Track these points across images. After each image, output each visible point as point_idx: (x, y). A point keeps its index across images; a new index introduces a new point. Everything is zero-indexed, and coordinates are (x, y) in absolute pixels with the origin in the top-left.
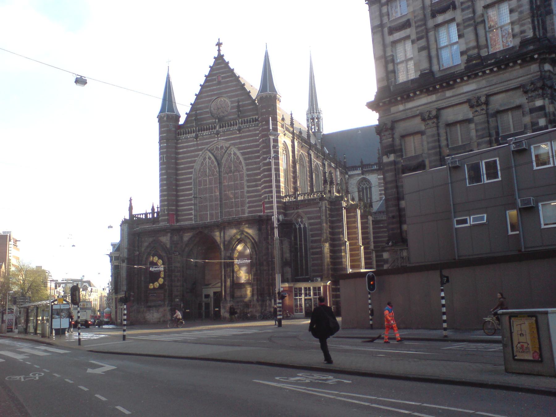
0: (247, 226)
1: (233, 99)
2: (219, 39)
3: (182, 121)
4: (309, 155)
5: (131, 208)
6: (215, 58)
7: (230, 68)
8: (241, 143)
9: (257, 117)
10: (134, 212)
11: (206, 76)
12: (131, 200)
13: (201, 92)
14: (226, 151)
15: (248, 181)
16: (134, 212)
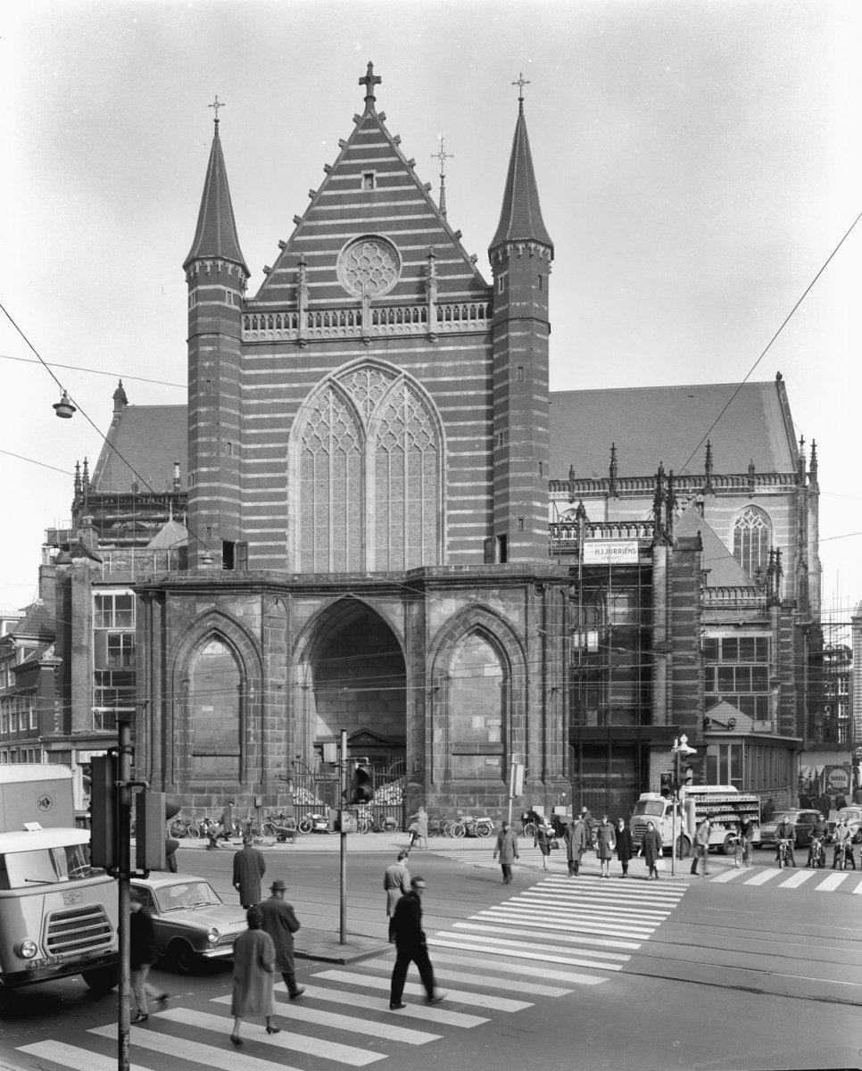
1: (410, 248)
2: (370, 65)
3: (253, 288)
13: (311, 215)
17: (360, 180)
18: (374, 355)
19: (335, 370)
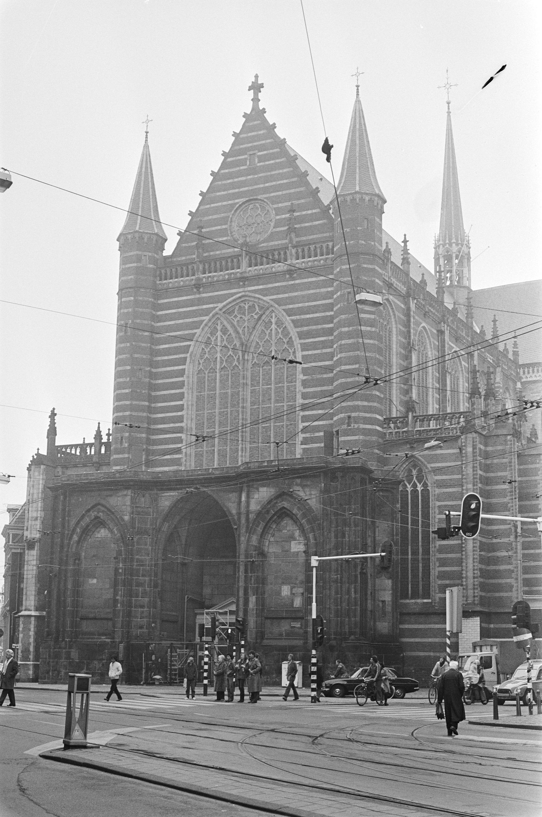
0: (298, 481)
2: (257, 77)
3: (169, 250)
4: (441, 332)
5: (52, 432)
6: (245, 115)
7: (277, 136)
8: (292, 301)
9: (330, 244)
10: (59, 441)
11: (224, 154)
12: (53, 415)
14: (259, 318)
15: (305, 384)
16: (59, 441)
17: (246, 159)
18: (249, 291)
19: (220, 305)
